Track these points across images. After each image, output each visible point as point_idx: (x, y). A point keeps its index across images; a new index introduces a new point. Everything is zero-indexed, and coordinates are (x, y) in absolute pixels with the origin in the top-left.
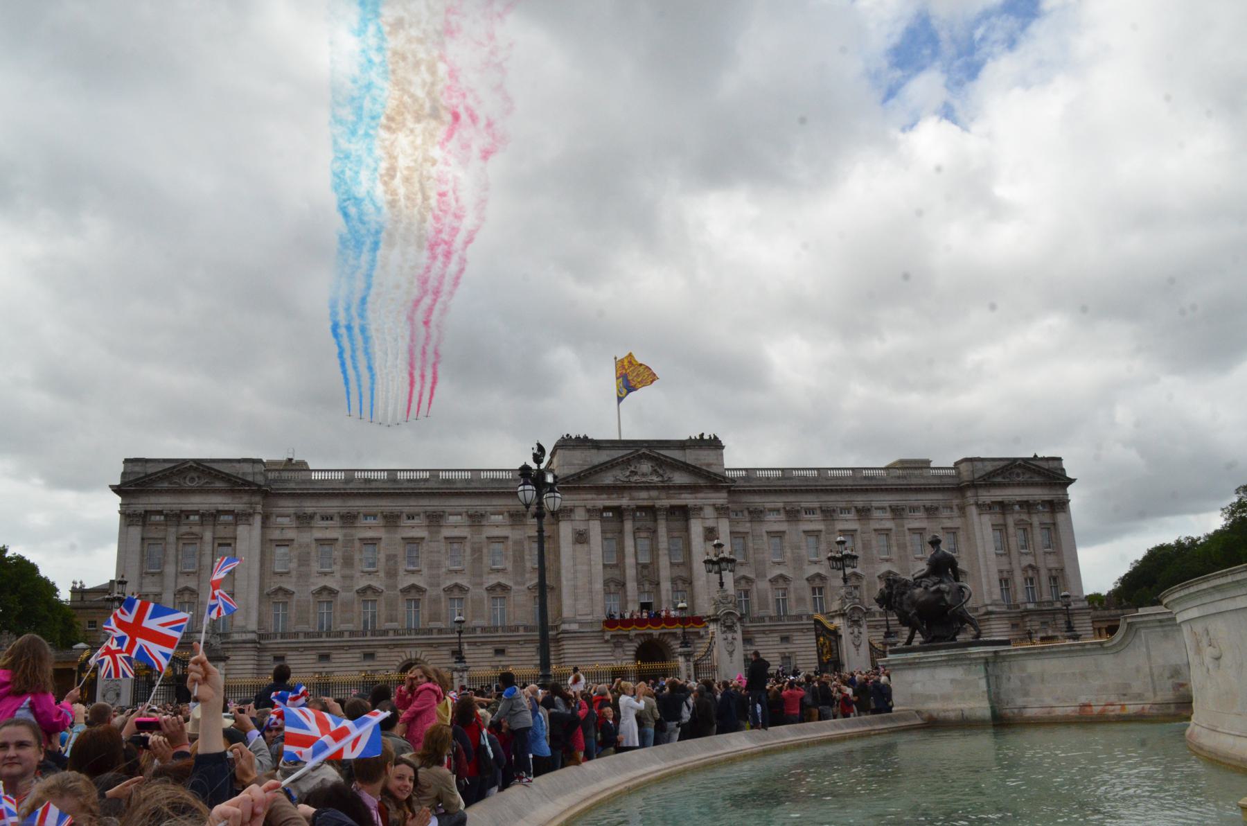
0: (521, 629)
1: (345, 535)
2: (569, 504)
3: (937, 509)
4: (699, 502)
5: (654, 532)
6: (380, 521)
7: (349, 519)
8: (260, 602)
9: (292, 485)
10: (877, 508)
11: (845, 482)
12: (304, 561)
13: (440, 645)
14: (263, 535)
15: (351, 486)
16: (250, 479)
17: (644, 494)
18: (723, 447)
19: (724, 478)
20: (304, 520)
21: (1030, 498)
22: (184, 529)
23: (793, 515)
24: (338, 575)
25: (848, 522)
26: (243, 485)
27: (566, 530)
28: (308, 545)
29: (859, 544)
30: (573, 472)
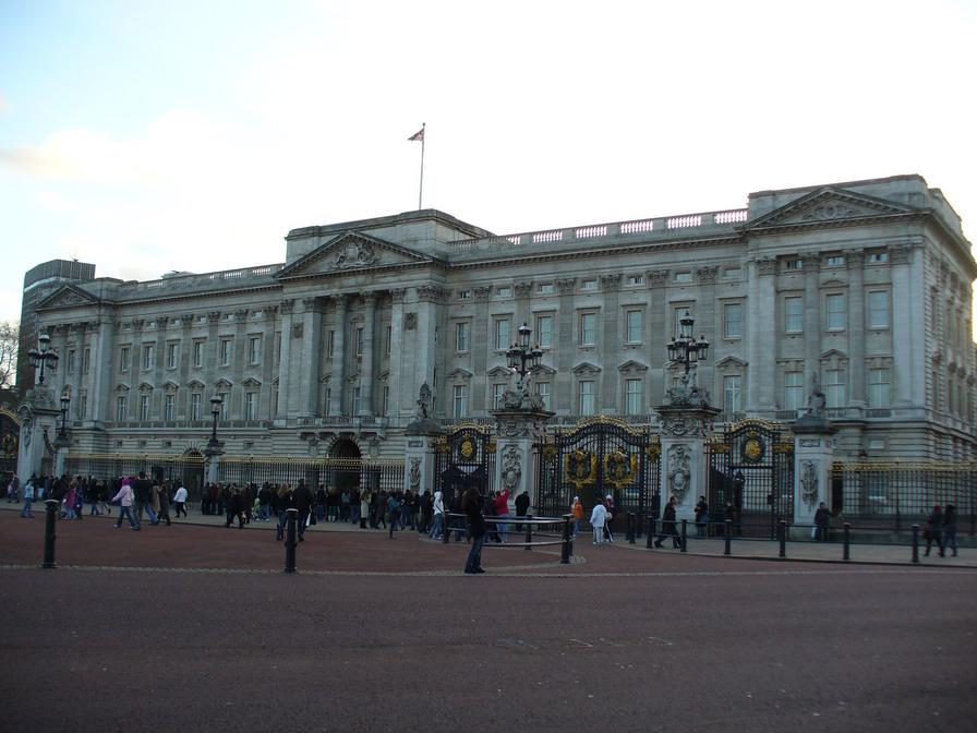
0: (261, 424)
1: (159, 338)
2: (289, 297)
3: (715, 271)
4: (400, 285)
8: (109, 396)
10: (630, 277)
11: (592, 244)
12: (136, 364)
15: (165, 293)
16: (98, 295)
17: (351, 281)
19: (421, 254)
21: (847, 247)
22: (70, 339)
24: (154, 373)
25: (591, 296)
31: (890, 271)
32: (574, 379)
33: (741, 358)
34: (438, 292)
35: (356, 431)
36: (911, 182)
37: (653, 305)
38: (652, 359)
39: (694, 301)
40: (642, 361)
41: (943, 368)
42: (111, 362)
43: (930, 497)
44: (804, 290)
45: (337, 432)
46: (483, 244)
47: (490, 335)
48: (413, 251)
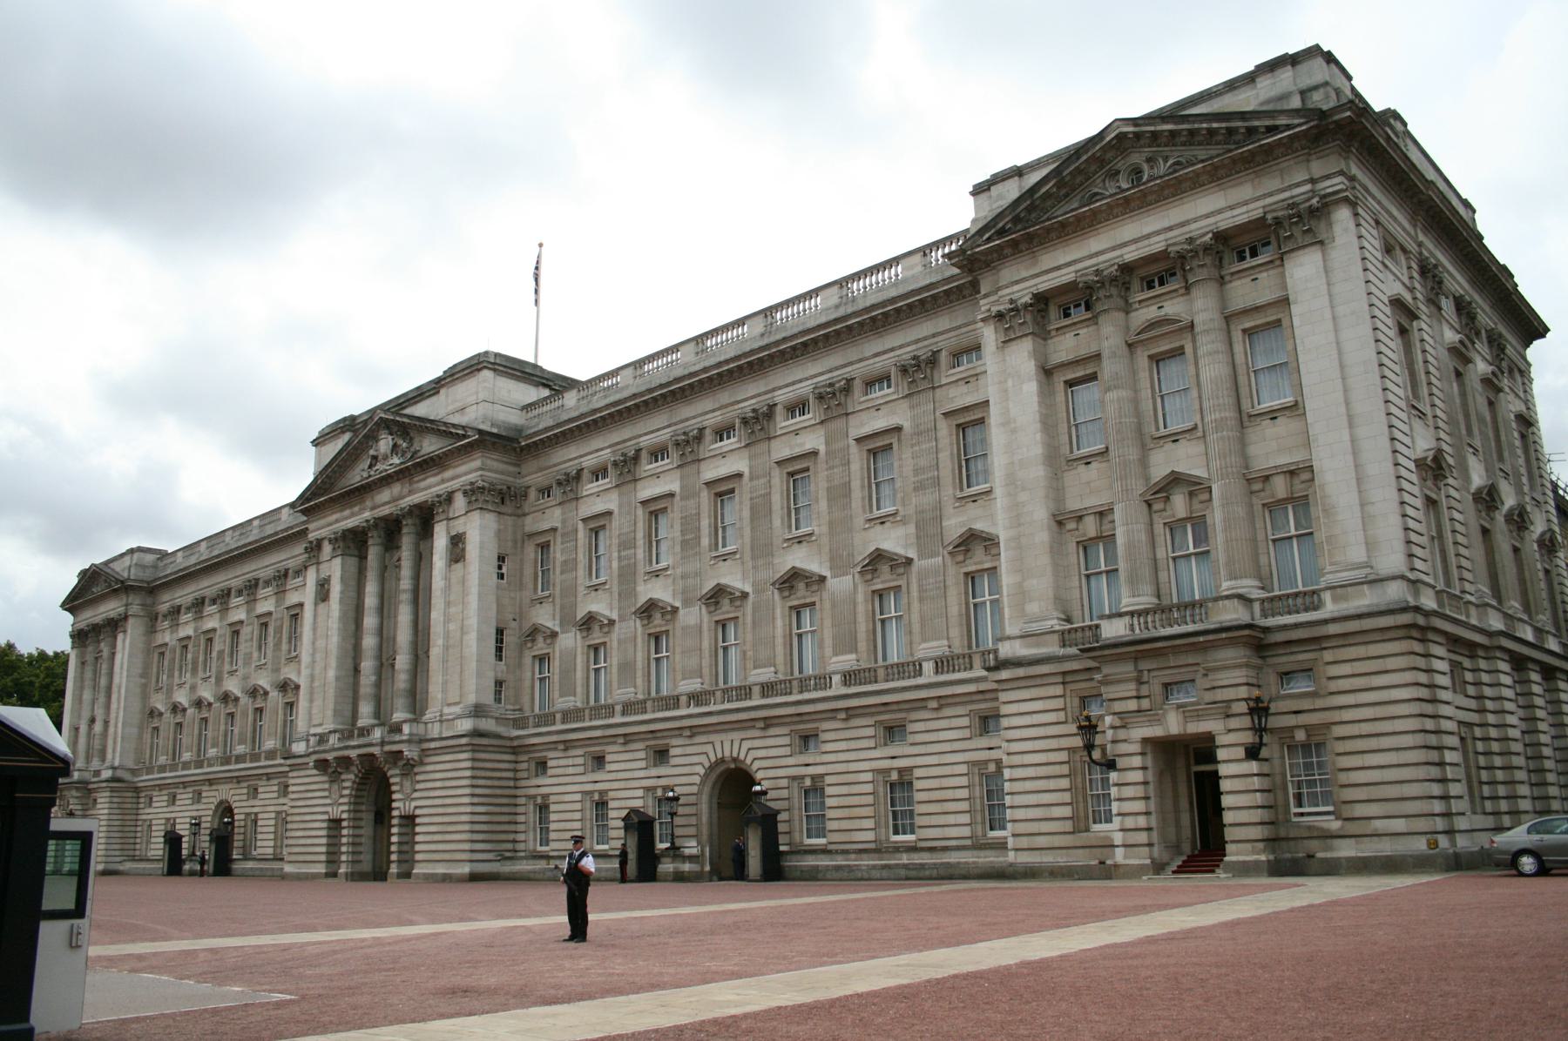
3: (933, 361)
12: (171, 671)
13: (239, 780)
14: (148, 642)
17: (384, 495)
19: (463, 428)
31: (1283, 275)
32: (706, 618)
33: (992, 530)
34: (500, 492)
35: (376, 750)
36: (1303, 68)
37: (827, 453)
38: (832, 559)
39: (898, 429)
40: (815, 566)
41: (1457, 496)
42: (142, 676)
43: (1456, 806)
44: (1097, 357)
45: (353, 754)
46: (570, 399)
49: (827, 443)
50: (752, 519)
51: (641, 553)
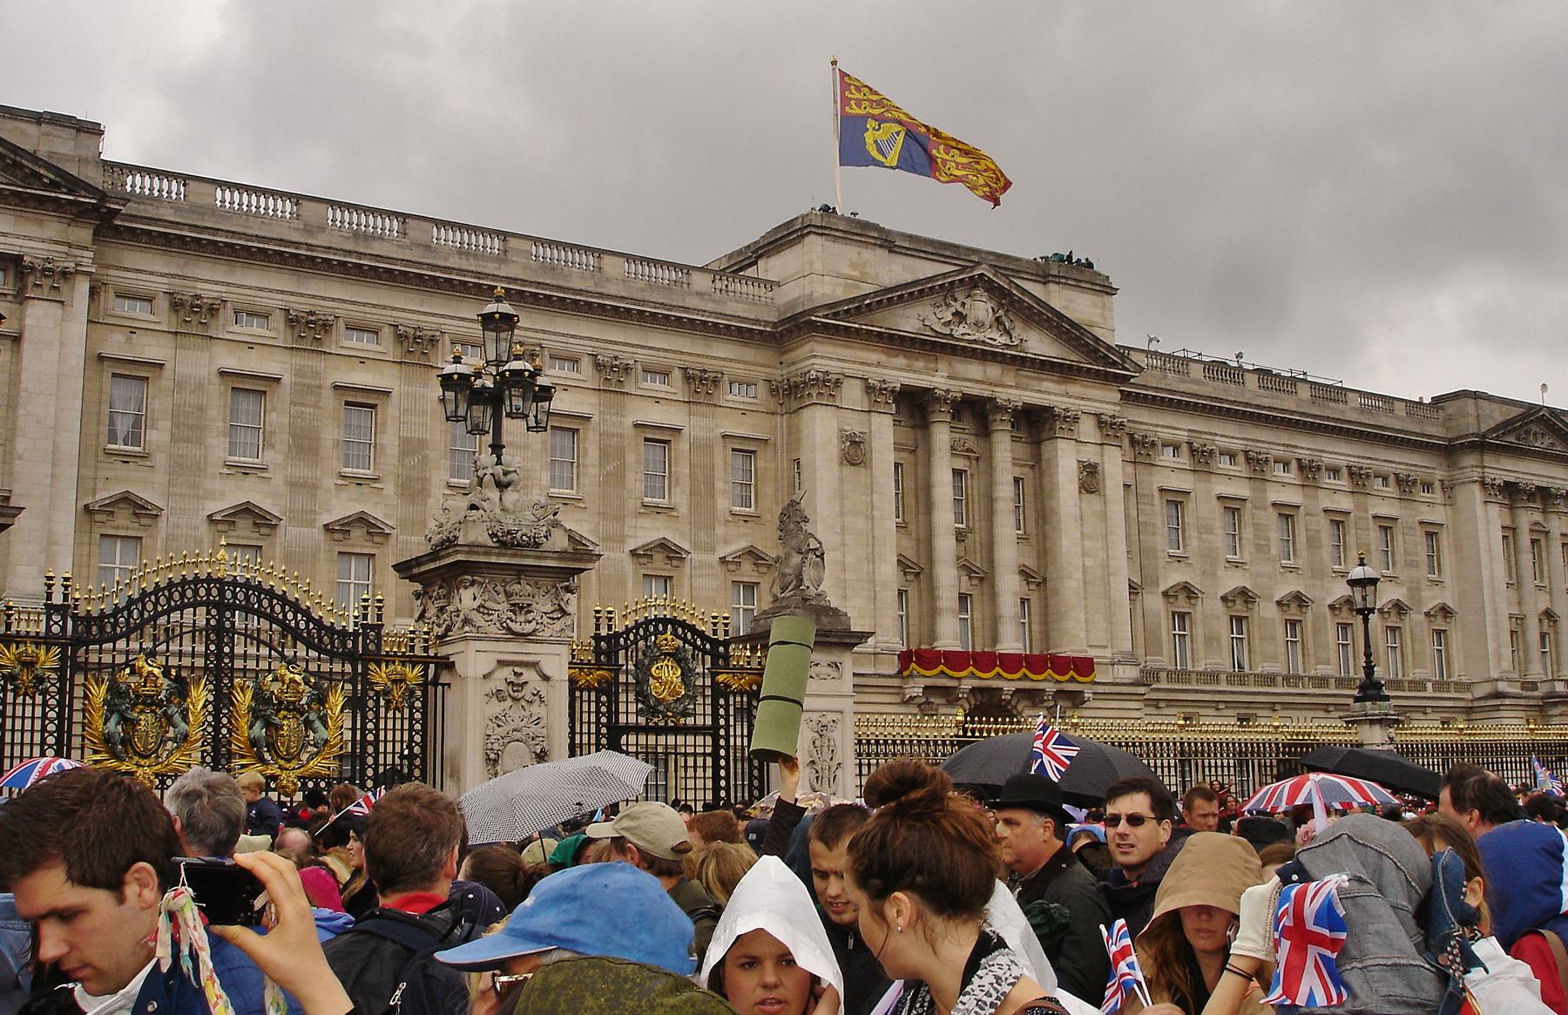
1: (299, 372)
2: (834, 367)
3: (1415, 482)
4: (1073, 404)
5: (985, 460)
6: (386, 346)
7: (309, 329)
9: (168, 215)
12: (188, 428)
17: (974, 369)
18: (1110, 291)
20: (194, 314)
21: (1554, 484)
23: (1202, 458)
24: (278, 478)
26: (54, 185)
27: (822, 428)
28: (200, 387)
29: (1301, 538)
30: (840, 294)
47: (1159, 523)
48: (1109, 348)
49: (1357, 507)
50: (1309, 547)
51: (1220, 540)
